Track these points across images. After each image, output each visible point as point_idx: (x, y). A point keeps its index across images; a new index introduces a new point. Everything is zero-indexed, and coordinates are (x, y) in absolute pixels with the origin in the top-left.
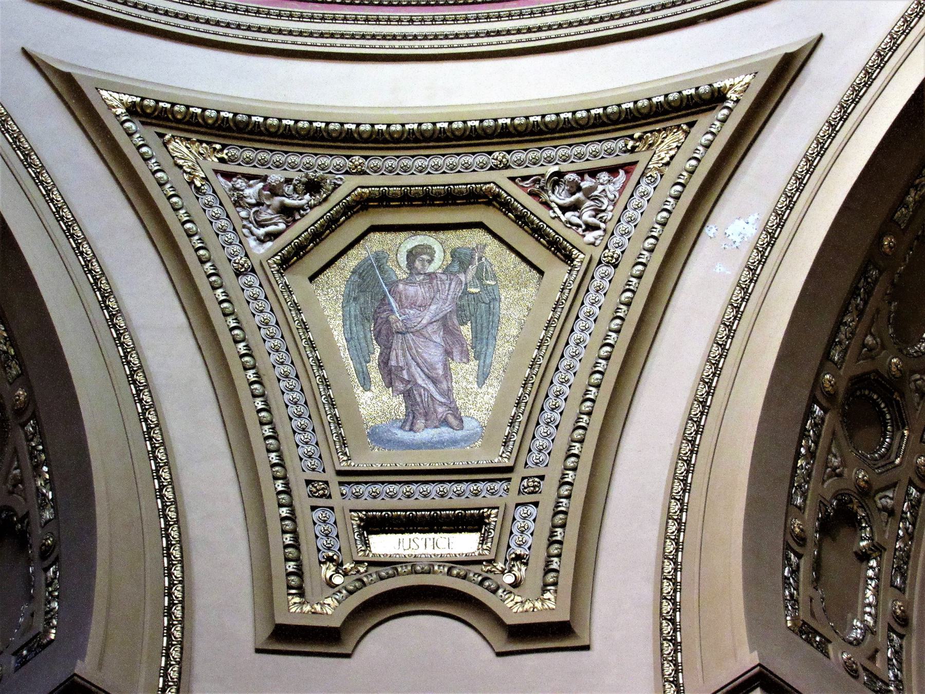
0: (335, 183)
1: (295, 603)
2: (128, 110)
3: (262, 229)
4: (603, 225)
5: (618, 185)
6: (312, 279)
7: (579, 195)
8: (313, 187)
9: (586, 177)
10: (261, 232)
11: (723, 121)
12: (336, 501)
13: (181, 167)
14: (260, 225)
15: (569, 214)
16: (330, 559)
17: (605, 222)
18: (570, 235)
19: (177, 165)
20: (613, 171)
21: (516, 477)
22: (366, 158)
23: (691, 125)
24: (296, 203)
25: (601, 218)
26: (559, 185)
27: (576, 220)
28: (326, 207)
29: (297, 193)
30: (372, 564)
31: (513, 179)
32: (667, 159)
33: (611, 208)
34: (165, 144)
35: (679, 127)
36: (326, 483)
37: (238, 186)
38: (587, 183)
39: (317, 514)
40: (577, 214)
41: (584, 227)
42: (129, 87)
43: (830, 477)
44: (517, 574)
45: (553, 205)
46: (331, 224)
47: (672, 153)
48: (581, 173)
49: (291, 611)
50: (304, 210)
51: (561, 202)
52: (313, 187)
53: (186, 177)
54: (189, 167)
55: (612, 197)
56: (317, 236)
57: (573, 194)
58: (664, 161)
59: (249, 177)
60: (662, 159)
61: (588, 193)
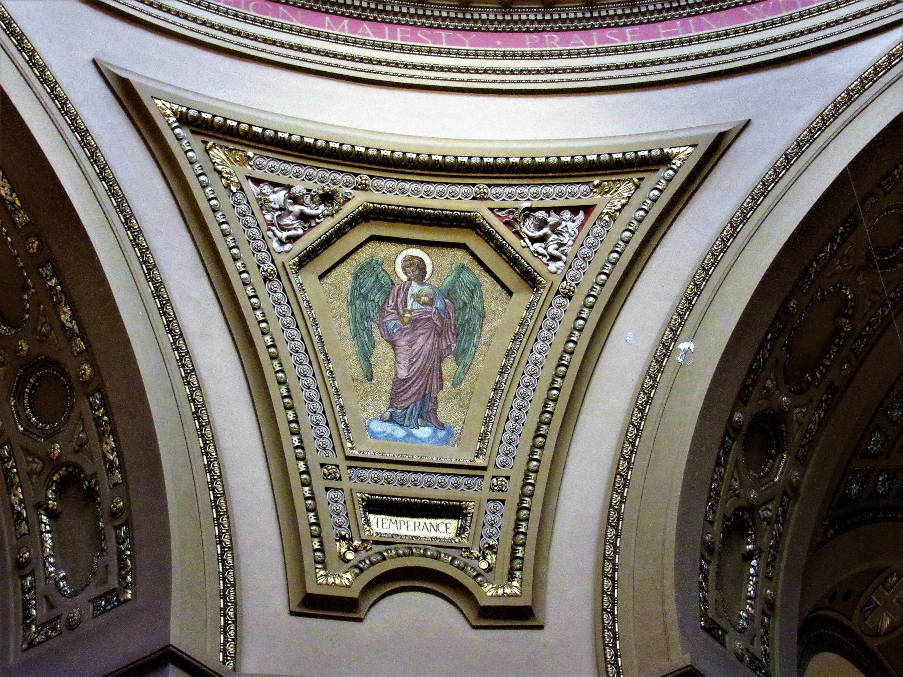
0: (346, 198)
1: (322, 575)
2: (178, 120)
3: (284, 232)
4: (564, 258)
5: (578, 223)
6: (321, 277)
7: (546, 230)
8: (327, 198)
9: (552, 213)
10: (284, 235)
11: (669, 181)
12: (345, 484)
13: (220, 172)
14: (283, 229)
16: (343, 538)
17: (566, 255)
18: (536, 264)
19: (216, 170)
20: (575, 210)
22: (371, 177)
23: (641, 179)
24: (314, 212)
25: (563, 250)
26: (529, 217)
27: (542, 251)
28: (338, 217)
29: (313, 203)
30: (376, 543)
31: (491, 210)
32: (619, 207)
33: (571, 243)
34: (207, 151)
35: (630, 180)
36: (337, 466)
37: (264, 191)
38: (553, 219)
39: (331, 494)
40: (543, 245)
41: (548, 257)
42: (180, 98)
43: (731, 497)
44: (490, 561)
45: (524, 235)
46: (339, 232)
47: (624, 201)
48: (547, 210)
49: (319, 582)
50: (319, 218)
51: (531, 234)
52: (327, 198)
53: (224, 181)
54: (227, 173)
55: (572, 233)
56: (327, 243)
57: (540, 228)
58: (616, 208)
59: (274, 185)
60: (614, 206)
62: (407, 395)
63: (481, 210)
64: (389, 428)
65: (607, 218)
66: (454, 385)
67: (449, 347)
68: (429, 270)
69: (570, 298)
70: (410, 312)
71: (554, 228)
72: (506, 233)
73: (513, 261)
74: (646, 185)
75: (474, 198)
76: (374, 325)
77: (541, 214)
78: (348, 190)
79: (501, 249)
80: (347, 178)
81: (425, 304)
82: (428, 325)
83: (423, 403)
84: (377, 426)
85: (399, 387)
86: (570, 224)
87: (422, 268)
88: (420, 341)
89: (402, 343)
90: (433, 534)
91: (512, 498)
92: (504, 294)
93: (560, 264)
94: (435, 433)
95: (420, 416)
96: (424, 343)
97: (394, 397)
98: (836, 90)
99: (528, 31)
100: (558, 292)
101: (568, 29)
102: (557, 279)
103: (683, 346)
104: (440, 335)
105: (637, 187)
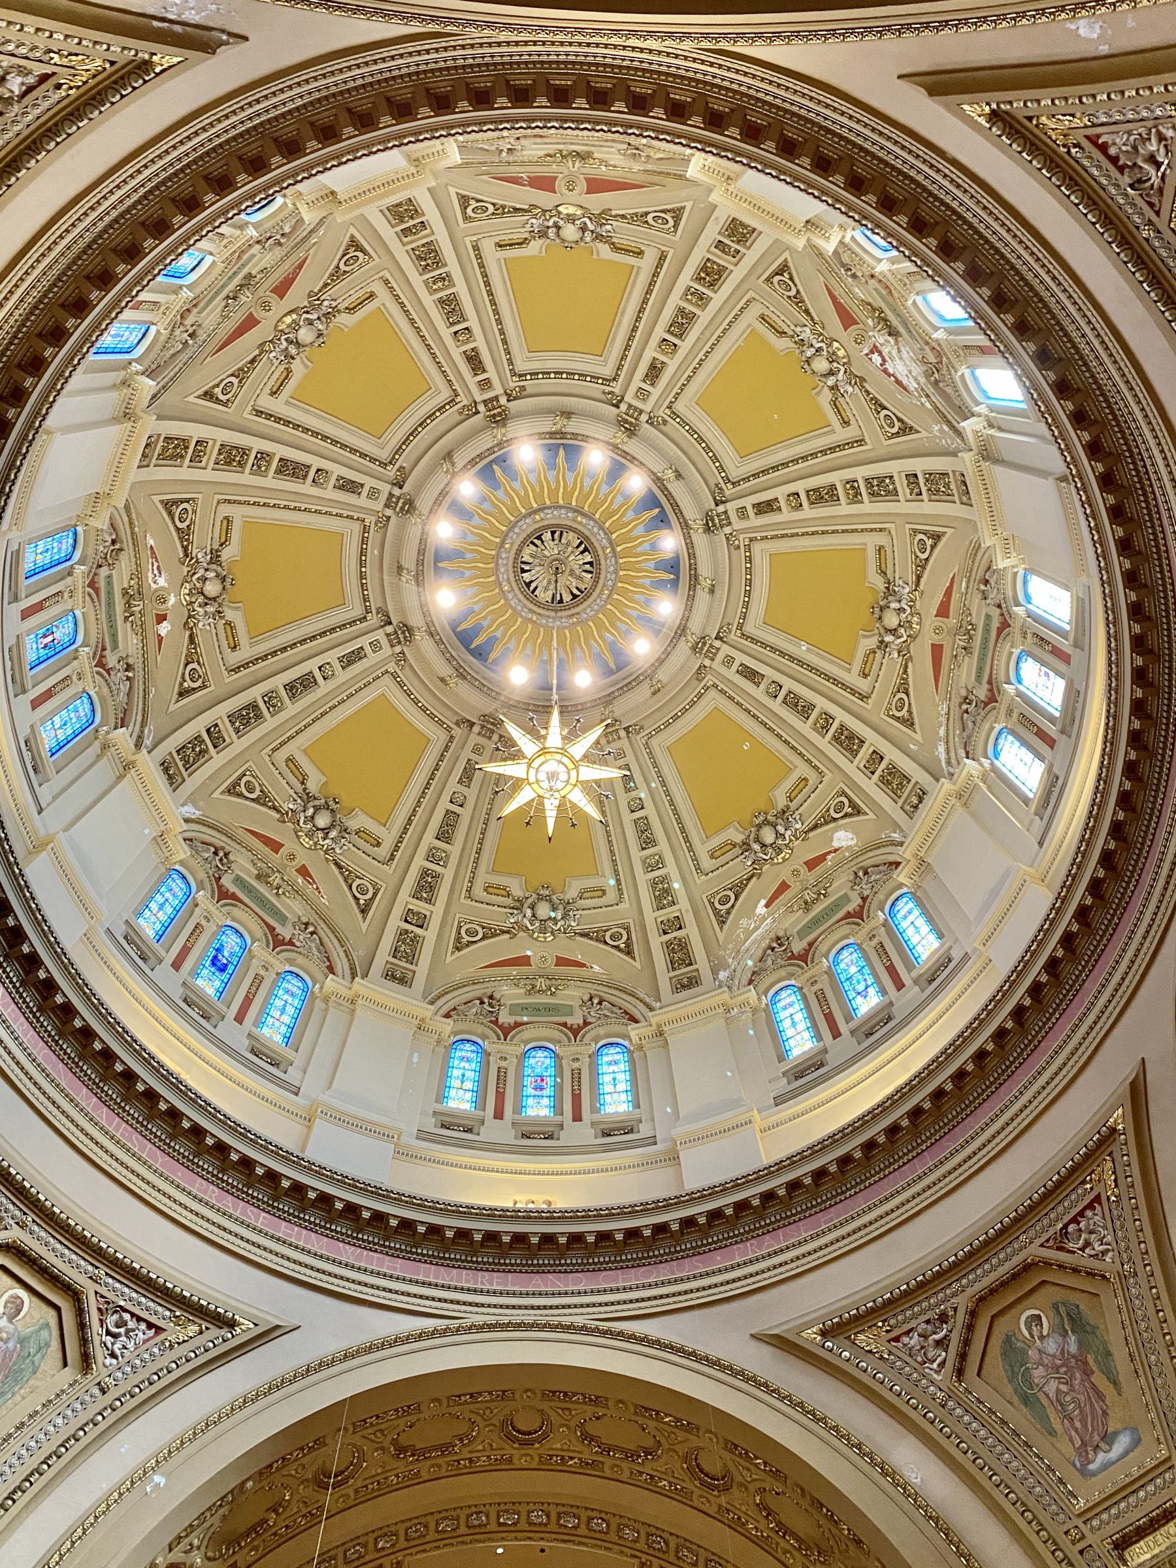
5: (146, 1337)
7: (122, 1330)
15: (109, 1338)
18: (99, 1353)
20: (150, 1325)
23: (207, 1328)
27: (109, 1345)
31: (96, 1293)
35: (200, 1325)
38: (132, 1324)
48: (133, 1315)
57: (118, 1327)
63: (89, 1289)
65: (167, 1344)
68: (22, 1313)
69: (104, 1393)
72: (95, 1317)
73: (84, 1341)
75: (91, 1278)
77: (127, 1316)
78: (12, 1222)
79: (82, 1326)
80: (18, 1213)
86: (141, 1335)
92: (60, 1363)
93: (114, 1361)
98: (364, 1339)
99: (202, 1177)
100: (99, 1384)
101: (227, 1191)
102: (105, 1372)
103: (158, 1478)
105: (201, 1332)
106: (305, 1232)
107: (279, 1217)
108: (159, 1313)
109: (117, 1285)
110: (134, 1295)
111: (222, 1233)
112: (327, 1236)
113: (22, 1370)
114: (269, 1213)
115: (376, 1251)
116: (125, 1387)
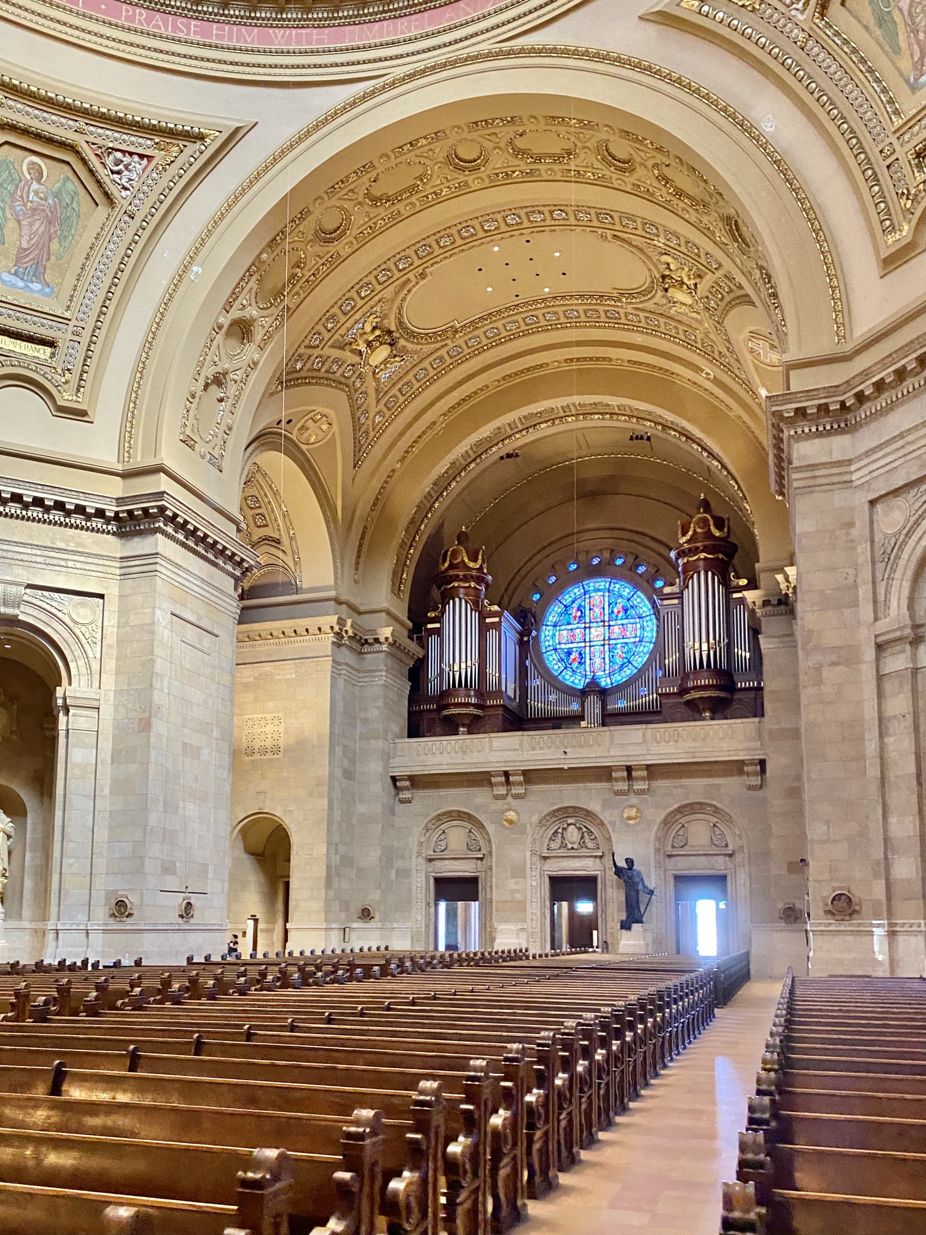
5: (143, 166)
7: (121, 167)
15: (115, 175)
18: (113, 190)
20: (142, 156)
21: (71, 323)
27: (119, 181)
31: (87, 142)
35: (178, 145)
38: (127, 159)
57: (117, 165)
61: (126, 167)
62: (27, 259)
64: (14, 279)
65: (160, 168)
66: (57, 259)
67: (56, 232)
68: (45, 174)
69: (133, 218)
70: (31, 202)
71: (126, 167)
74: (188, 151)
75: (76, 131)
76: (7, 207)
77: (119, 155)
79: (92, 172)
81: (41, 198)
82: (43, 214)
83: (37, 267)
84: (6, 277)
85: (22, 253)
86: (137, 165)
87: (41, 173)
88: (37, 224)
89: (24, 223)
90: (36, 354)
91: (85, 340)
93: (128, 193)
94: (43, 289)
95: (34, 275)
96: (39, 227)
97: (18, 260)
102: (126, 203)
104: (50, 223)
106: (235, 28)
107: (208, 20)
108: (144, 144)
109: (100, 131)
110: (116, 135)
111: (161, 56)
112: (256, 26)
113: (69, 217)
114: (197, 18)
115: (303, 27)
116: (145, 210)
